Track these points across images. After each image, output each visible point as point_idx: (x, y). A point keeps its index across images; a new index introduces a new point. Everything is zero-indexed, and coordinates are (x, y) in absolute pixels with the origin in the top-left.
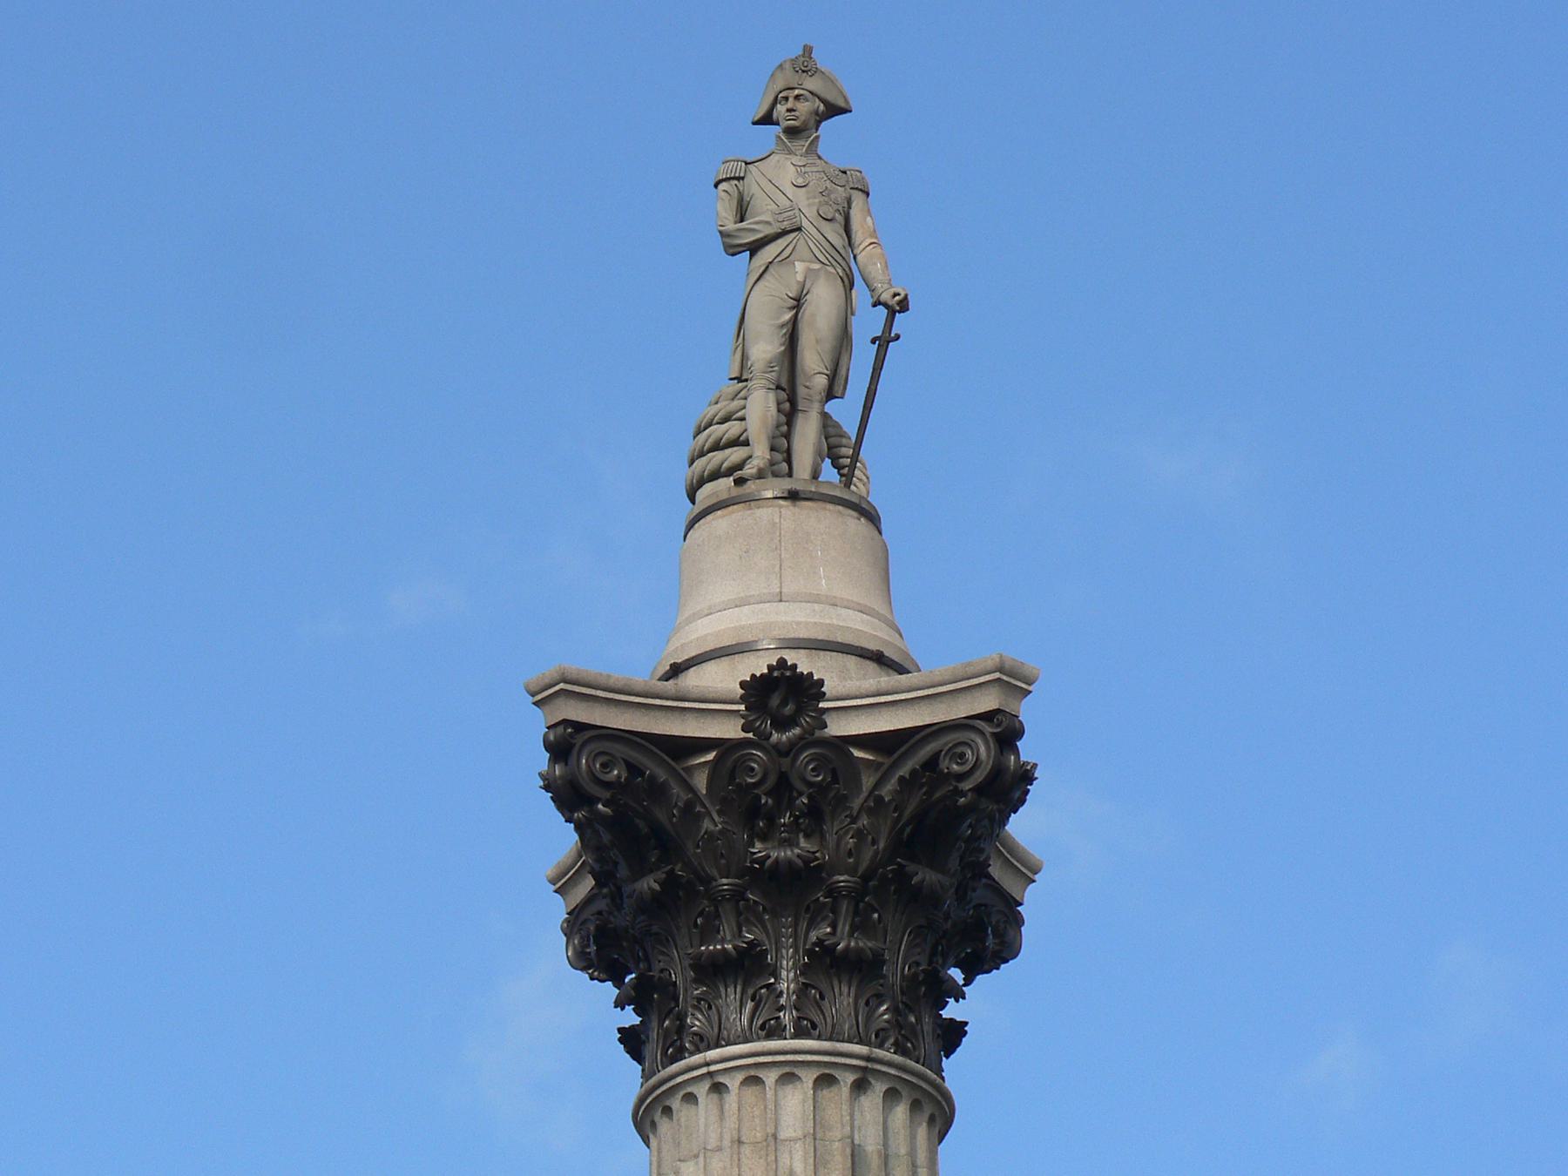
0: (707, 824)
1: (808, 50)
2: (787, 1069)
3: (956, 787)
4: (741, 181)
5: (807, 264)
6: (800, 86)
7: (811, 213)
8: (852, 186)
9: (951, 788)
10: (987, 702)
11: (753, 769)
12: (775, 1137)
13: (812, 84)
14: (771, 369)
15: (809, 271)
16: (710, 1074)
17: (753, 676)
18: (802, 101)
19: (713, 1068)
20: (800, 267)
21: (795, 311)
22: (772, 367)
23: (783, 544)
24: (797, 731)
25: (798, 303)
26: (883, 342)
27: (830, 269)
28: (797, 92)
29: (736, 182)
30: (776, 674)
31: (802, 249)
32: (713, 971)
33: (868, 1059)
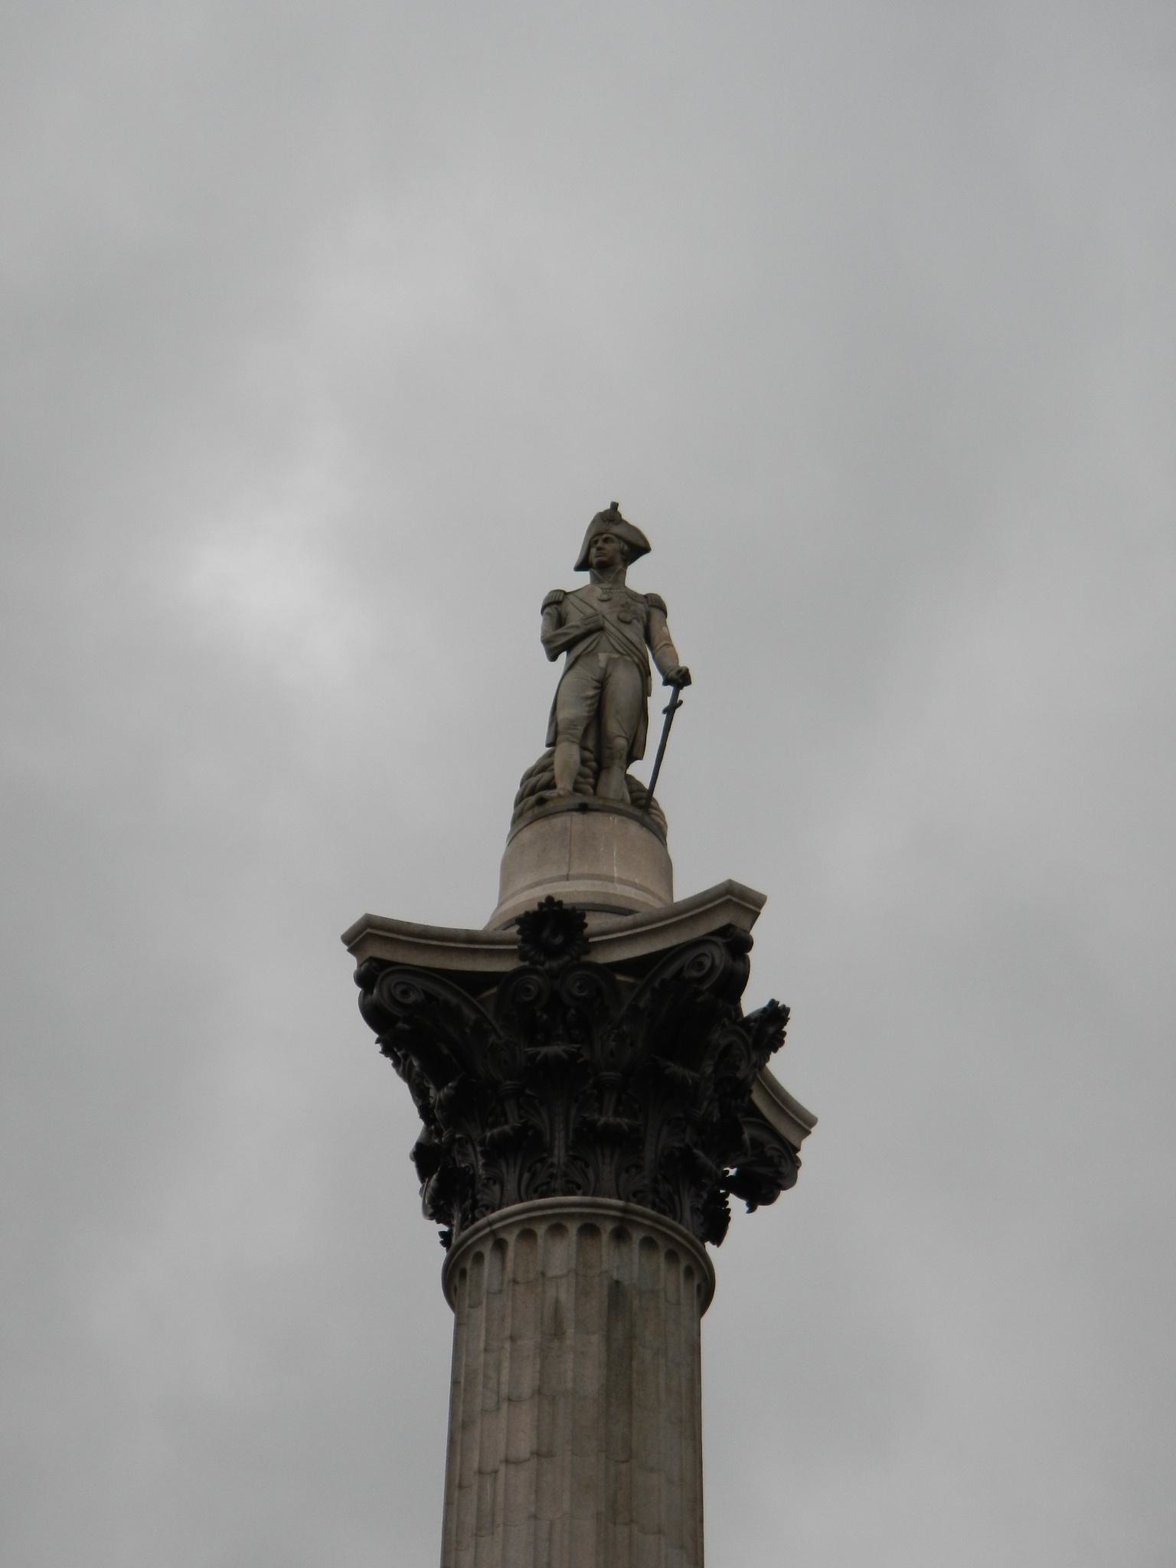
0: (492, 1038)
1: (615, 506)
2: (554, 1221)
6: (607, 532)
7: (612, 618)
8: (650, 603)
10: (719, 921)
11: (529, 990)
12: (543, 1274)
13: (617, 529)
15: (610, 660)
16: (493, 1232)
19: (495, 1226)
24: (567, 958)
25: (602, 684)
26: (670, 711)
27: (628, 658)
28: (604, 536)
30: (545, 909)
32: (496, 1152)
33: (624, 1210)
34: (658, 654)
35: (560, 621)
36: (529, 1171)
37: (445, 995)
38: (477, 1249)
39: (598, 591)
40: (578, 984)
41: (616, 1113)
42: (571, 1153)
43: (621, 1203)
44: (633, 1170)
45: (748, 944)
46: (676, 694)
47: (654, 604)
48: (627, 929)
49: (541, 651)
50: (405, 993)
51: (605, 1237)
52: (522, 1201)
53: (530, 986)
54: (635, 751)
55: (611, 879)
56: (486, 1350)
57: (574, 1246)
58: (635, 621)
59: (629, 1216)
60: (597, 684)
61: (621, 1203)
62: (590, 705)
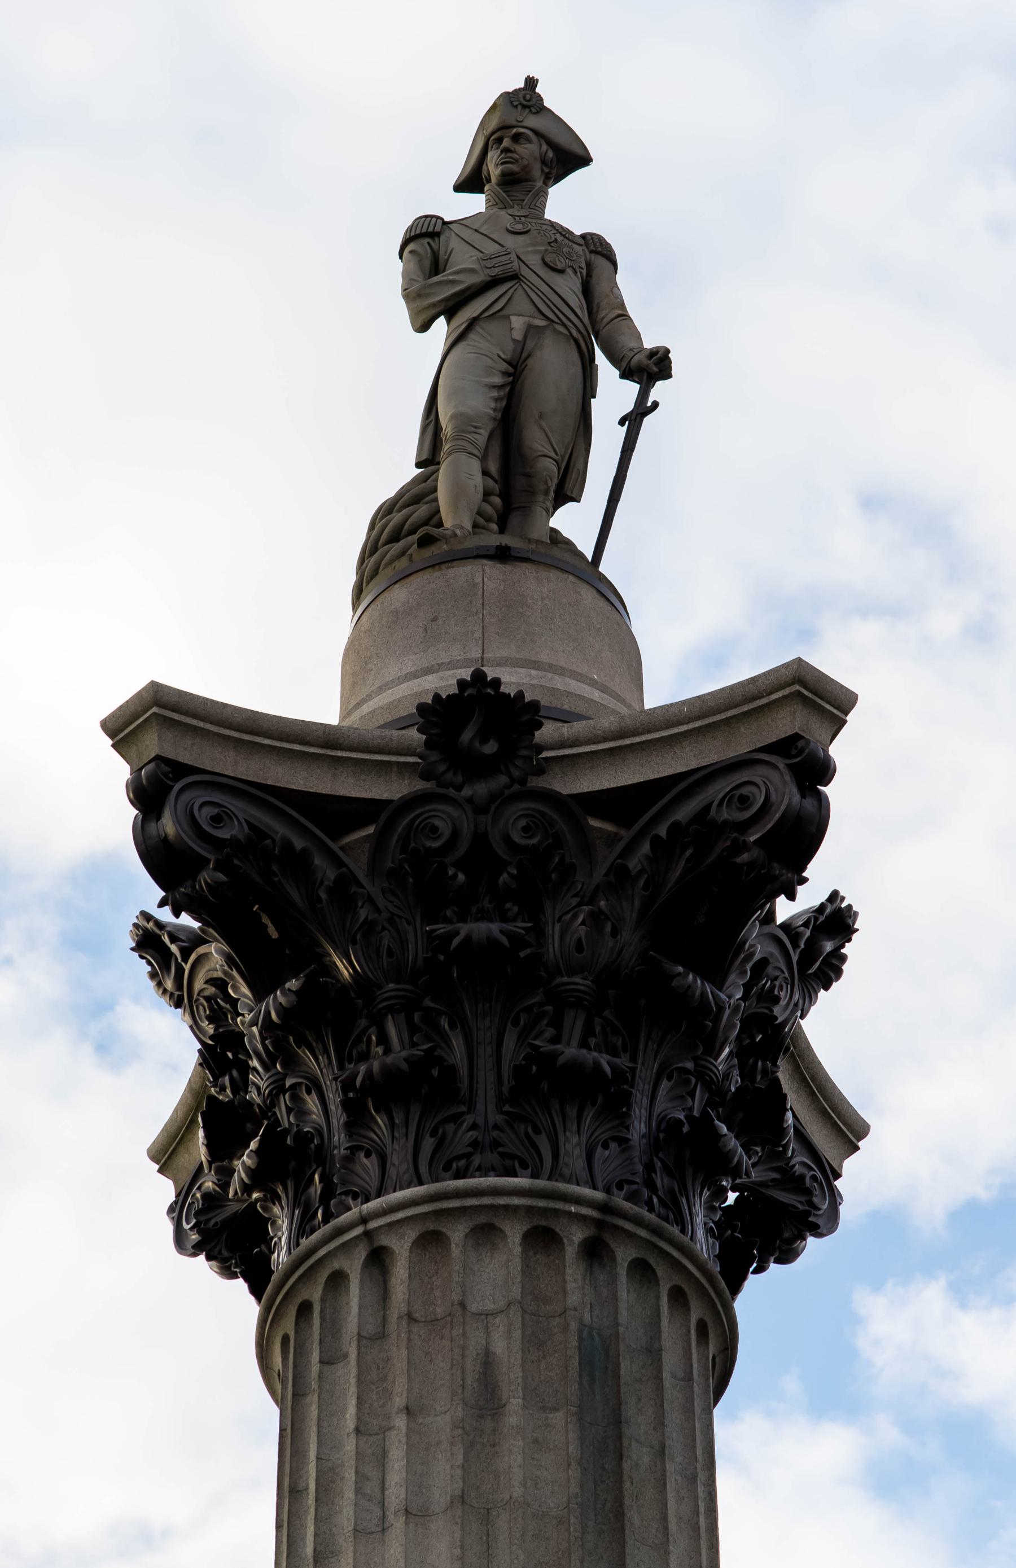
0: (363, 913)
1: (531, 83)
2: (482, 1219)
3: (735, 841)
4: (436, 239)
5: (527, 319)
7: (534, 261)
8: (592, 247)
9: (728, 843)
11: (434, 829)
12: (463, 1305)
13: (533, 121)
14: (473, 429)
15: (530, 330)
17: (437, 697)
18: (522, 141)
19: (373, 1225)
20: (518, 323)
21: (511, 379)
22: (476, 427)
23: (487, 607)
24: (503, 780)
29: (425, 241)
30: (469, 692)
31: (520, 301)
33: (605, 1208)
34: (603, 333)
35: (436, 266)
36: (433, 1135)
37: (280, 829)
38: (336, 1264)
39: (505, 218)
40: (523, 823)
41: (584, 1044)
42: (507, 1108)
43: (599, 1195)
44: (613, 1145)
45: (825, 771)
46: (643, 395)
47: (600, 249)
48: (605, 740)
49: (401, 312)
50: (216, 820)
51: (571, 1252)
52: (421, 1183)
53: (437, 822)
54: (569, 484)
55: (554, 669)
56: (357, 1431)
57: (517, 1261)
58: (569, 271)
59: (609, 1219)
60: (504, 366)
61: (599, 1195)
62: (497, 400)
